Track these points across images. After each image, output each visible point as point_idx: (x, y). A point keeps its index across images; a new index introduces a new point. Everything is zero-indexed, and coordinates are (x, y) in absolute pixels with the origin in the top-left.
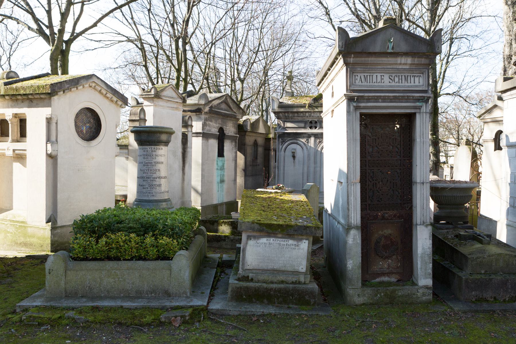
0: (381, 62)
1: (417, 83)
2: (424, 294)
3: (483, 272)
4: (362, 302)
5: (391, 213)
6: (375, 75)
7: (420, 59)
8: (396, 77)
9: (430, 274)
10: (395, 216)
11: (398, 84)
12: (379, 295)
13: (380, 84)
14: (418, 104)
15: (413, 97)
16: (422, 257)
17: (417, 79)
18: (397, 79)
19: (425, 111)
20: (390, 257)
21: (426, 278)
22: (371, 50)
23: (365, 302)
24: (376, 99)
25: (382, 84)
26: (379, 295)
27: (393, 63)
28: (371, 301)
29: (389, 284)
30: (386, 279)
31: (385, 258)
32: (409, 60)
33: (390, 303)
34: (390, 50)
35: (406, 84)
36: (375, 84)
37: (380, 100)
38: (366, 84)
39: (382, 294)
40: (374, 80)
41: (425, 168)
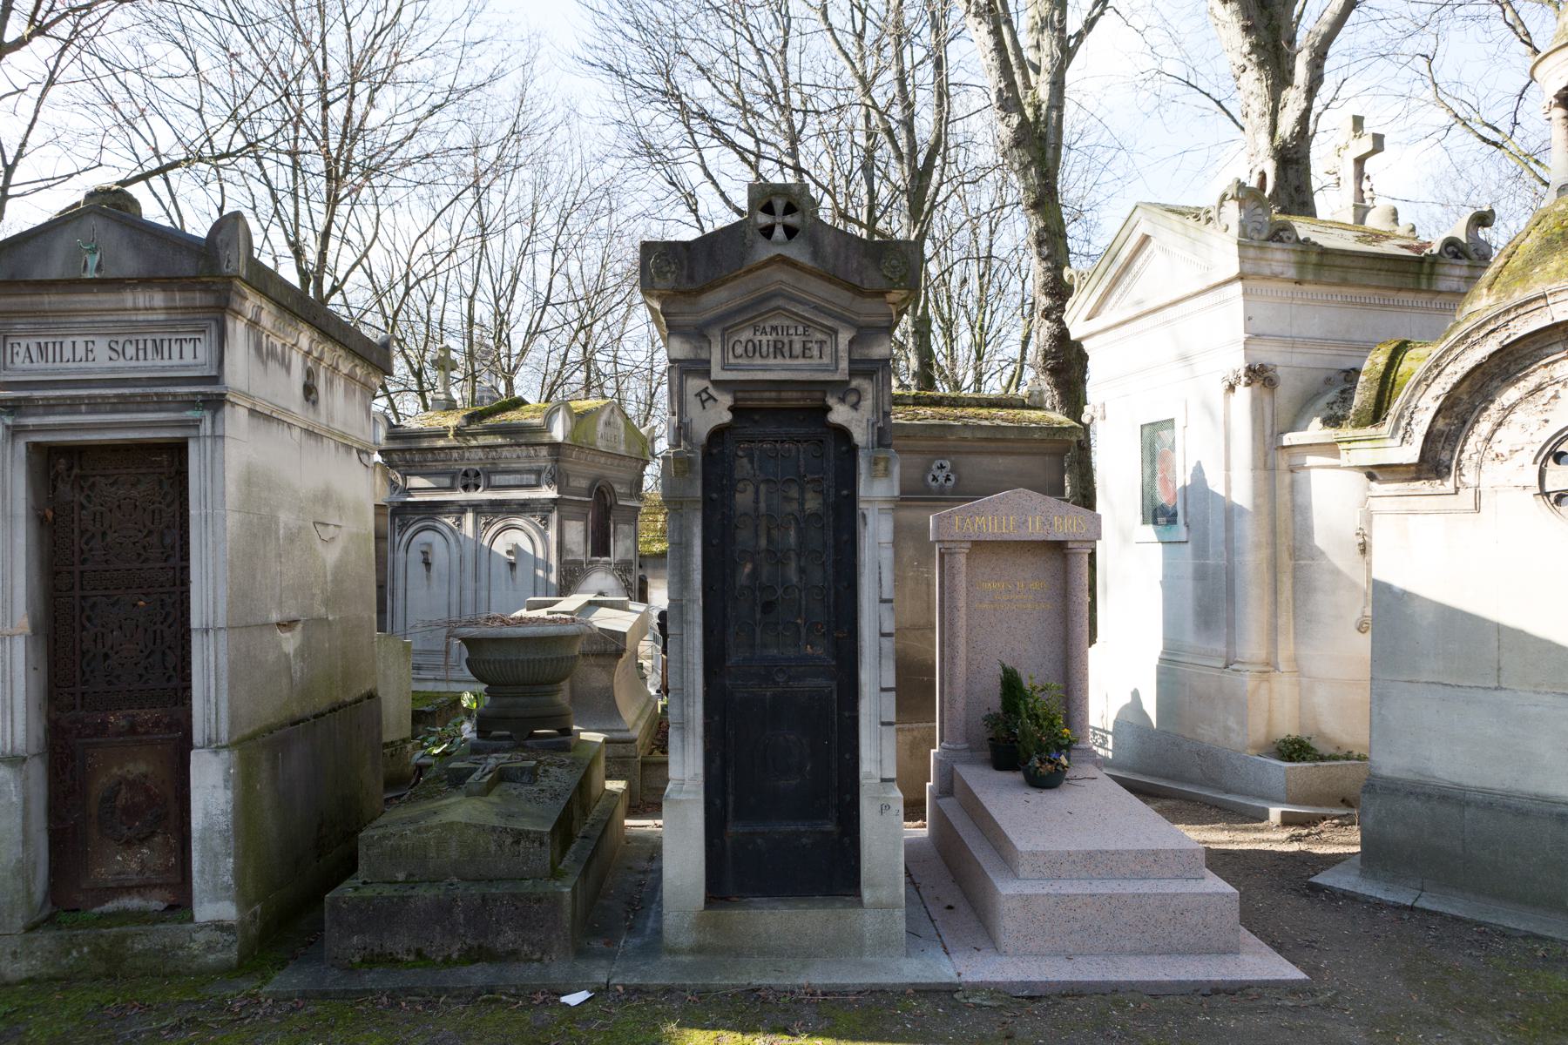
0: (79, 306)
1: (188, 357)
2: (210, 947)
3: (401, 876)
4: (24, 975)
5: (145, 715)
6: (68, 342)
7: (188, 295)
8: (128, 346)
9: (228, 888)
10: (156, 724)
11: (134, 363)
12: (75, 953)
13: (83, 364)
14: (190, 414)
15: (175, 395)
16: (202, 839)
17: (188, 348)
18: (130, 350)
19: (209, 432)
20: (145, 839)
21: (218, 899)
22: (37, 275)
23: (32, 974)
24: (72, 405)
25: (90, 364)
26: (75, 953)
27: (113, 306)
28: (52, 971)
29: (141, 917)
30: (134, 903)
31: (129, 843)
32: (158, 299)
33: (108, 976)
34: (91, 274)
35: (158, 362)
36: (70, 365)
37: (83, 408)
38: (42, 364)
39: (86, 950)
40: (68, 354)
41: (210, 586)
